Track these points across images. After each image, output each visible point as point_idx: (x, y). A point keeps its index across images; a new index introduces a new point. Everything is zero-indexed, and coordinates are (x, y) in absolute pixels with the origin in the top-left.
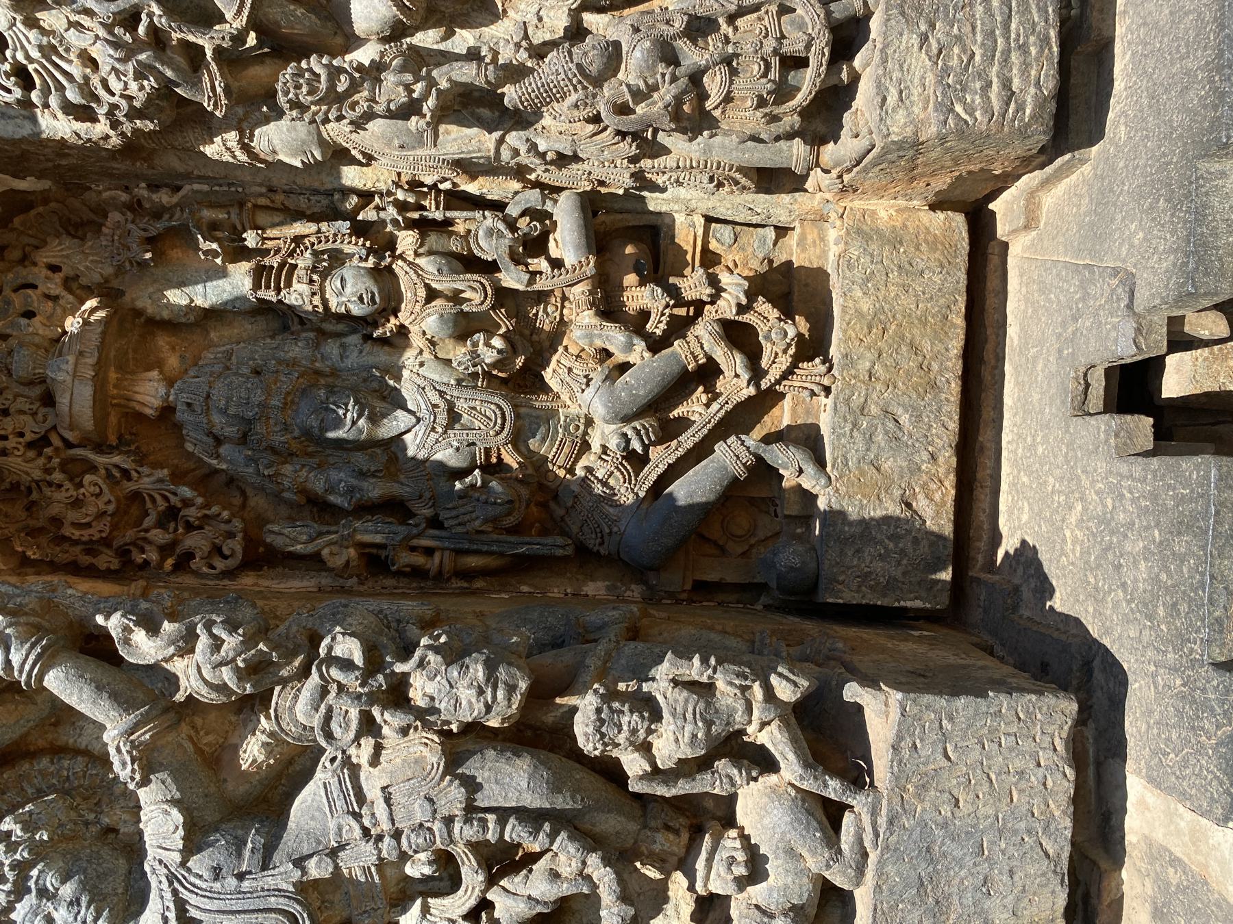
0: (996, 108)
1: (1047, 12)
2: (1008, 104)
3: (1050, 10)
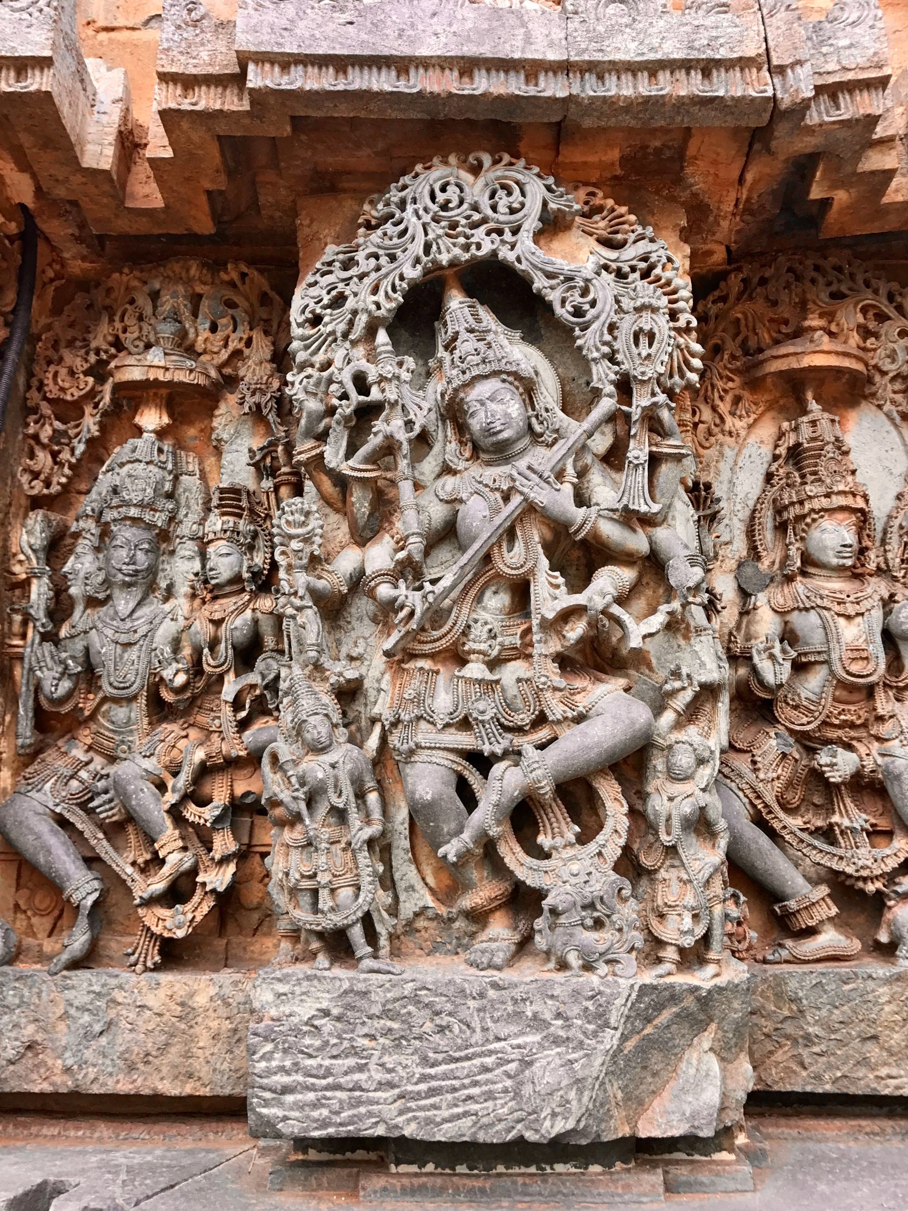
0: (265, 1081)
1: (349, 1124)
2: (270, 1090)
3: (351, 1128)
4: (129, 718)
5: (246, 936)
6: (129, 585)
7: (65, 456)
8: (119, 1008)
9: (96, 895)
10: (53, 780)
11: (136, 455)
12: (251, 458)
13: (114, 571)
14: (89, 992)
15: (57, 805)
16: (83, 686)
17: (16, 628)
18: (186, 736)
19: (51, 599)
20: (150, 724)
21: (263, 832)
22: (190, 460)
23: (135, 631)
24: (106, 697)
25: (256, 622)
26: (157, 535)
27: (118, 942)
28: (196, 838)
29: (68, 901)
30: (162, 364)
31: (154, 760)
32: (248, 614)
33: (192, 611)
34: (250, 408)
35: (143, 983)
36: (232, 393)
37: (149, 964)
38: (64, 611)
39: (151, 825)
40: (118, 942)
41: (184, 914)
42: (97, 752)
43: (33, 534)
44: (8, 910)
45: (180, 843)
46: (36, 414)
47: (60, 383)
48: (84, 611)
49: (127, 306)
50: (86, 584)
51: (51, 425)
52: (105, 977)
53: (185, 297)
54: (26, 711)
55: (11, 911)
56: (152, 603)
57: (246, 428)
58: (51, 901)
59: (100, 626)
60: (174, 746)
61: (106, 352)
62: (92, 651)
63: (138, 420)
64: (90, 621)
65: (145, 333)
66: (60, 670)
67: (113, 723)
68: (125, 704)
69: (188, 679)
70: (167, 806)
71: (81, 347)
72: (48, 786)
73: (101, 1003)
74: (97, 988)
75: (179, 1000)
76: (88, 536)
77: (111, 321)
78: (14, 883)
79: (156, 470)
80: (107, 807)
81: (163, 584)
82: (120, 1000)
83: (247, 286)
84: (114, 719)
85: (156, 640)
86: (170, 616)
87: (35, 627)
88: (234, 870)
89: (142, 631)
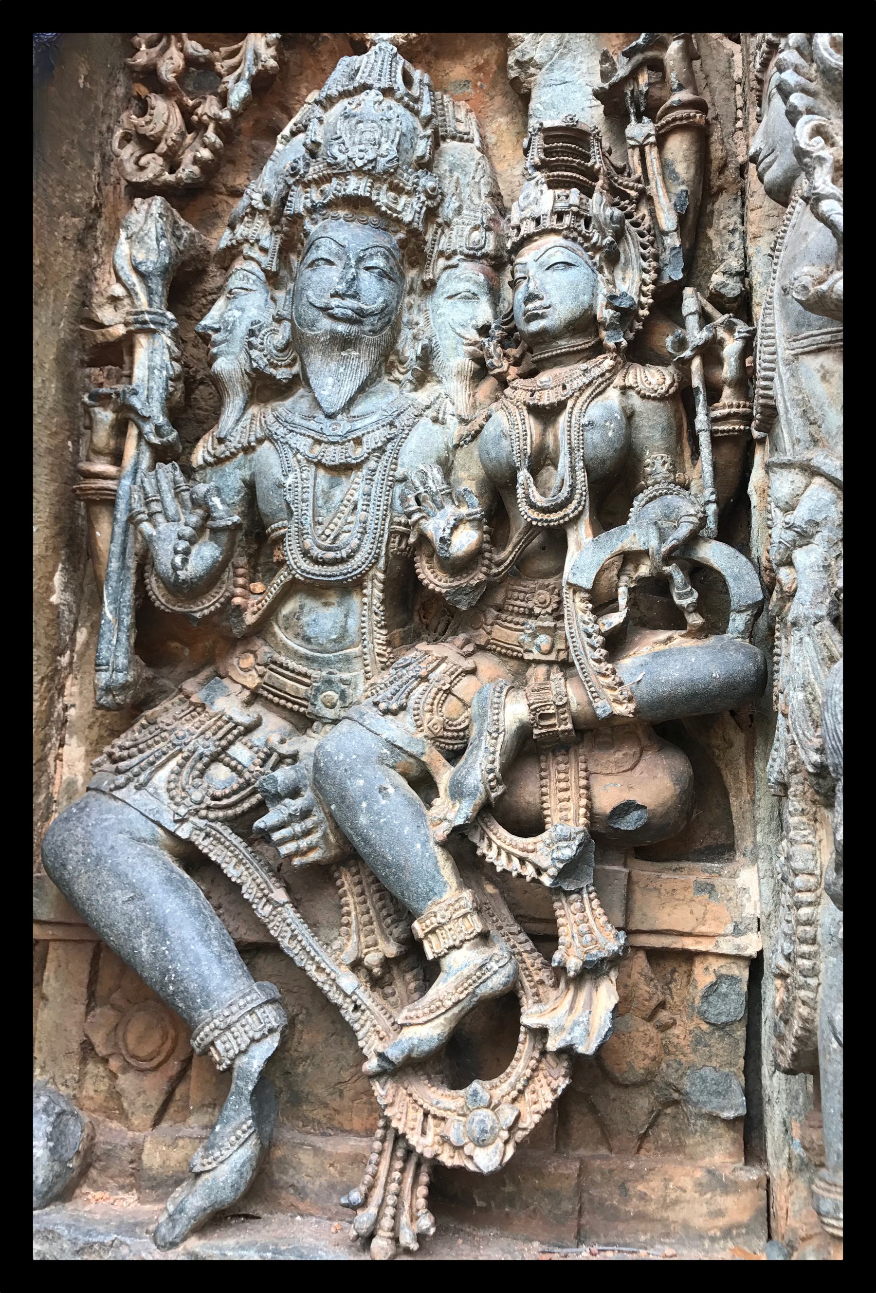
4: (344, 629)
5: (621, 1151)
6: (344, 343)
9: (272, 1043)
10: (173, 765)
15: (182, 821)
16: (243, 561)
17: (102, 437)
18: (473, 672)
19: (175, 379)
20: (389, 643)
21: (653, 899)
22: (461, 115)
23: (358, 441)
24: (294, 581)
25: (630, 416)
26: (400, 241)
27: (316, 1150)
28: (505, 911)
29: (206, 1052)
31: (406, 720)
32: (613, 396)
33: (474, 407)
38: (201, 422)
39: (407, 878)
41: (492, 1106)
42: (269, 704)
43: (141, 241)
44: (68, 1054)
45: (476, 925)
48: (245, 409)
50: (251, 345)
54: (117, 612)
55: (76, 1058)
56: (387, 391)
58: (164, 1037)
59: (281, 431)
60: (448, 692)
62: (263, 486)
64: (257, 427)
66: (194, 519)
67: (308, 640)
68: (334, 599)
69: (481, 541)
70: (442, 832)
72: (162, 777)
76: (256, 253)
78: (82, 991)
79: (400, 109)
80: (298, 828)
81: (411, 351)
84: (309, 632)
85: (404, 458)
86: (431, 413)
87: (141, 435)
88: (614, 1000)
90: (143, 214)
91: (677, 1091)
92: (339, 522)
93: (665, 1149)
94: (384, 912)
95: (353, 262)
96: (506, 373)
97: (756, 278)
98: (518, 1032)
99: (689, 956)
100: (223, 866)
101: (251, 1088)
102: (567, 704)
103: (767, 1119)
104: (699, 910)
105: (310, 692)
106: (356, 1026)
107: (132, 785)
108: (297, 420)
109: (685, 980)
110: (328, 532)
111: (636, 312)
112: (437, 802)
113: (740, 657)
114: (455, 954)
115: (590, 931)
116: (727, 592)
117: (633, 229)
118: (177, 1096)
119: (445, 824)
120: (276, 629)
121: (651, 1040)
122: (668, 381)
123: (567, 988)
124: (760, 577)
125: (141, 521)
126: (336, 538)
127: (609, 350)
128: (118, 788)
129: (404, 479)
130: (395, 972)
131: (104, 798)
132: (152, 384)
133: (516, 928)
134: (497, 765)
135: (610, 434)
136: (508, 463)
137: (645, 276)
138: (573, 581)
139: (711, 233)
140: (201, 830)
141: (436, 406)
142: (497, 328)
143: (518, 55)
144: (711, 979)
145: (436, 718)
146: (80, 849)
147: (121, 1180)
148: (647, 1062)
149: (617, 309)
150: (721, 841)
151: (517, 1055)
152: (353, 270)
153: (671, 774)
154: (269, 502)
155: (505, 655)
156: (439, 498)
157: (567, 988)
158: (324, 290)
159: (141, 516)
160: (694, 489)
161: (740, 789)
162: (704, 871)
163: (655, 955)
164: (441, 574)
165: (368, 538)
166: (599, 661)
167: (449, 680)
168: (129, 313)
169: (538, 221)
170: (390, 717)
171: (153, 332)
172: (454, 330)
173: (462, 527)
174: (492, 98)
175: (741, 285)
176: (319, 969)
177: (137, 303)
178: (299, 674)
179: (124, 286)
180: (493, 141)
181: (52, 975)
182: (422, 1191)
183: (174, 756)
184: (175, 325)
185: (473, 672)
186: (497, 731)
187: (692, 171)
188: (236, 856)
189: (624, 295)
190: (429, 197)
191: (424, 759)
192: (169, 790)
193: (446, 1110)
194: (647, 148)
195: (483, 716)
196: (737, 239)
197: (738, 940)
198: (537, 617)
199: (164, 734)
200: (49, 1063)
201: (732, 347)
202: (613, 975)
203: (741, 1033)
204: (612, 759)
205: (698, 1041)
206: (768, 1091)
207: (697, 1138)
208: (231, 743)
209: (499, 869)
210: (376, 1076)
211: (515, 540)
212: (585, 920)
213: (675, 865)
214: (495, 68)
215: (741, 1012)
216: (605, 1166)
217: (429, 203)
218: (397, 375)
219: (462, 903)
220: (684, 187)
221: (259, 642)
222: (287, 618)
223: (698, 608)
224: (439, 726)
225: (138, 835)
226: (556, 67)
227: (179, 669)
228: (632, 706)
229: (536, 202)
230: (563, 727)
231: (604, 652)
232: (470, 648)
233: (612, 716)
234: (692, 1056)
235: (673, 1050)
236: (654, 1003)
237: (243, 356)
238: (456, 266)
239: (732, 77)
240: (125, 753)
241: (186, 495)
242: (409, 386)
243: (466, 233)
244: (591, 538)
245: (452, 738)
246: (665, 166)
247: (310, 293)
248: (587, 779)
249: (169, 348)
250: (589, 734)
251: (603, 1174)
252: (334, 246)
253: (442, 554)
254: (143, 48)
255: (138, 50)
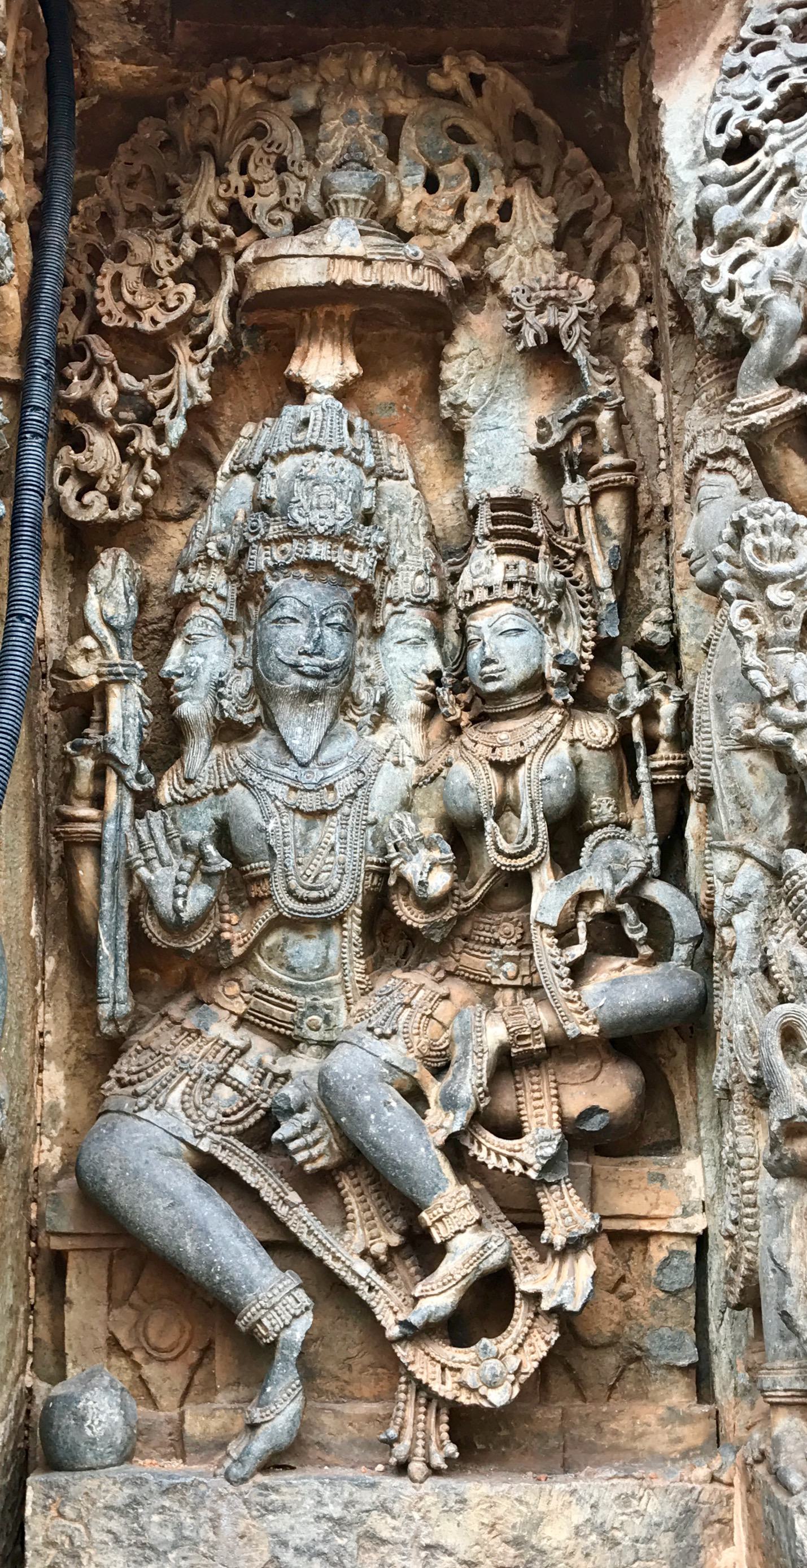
4: (326, 959)
5: (594, 1400)
6: (312, 696)
7: (145, 441)
8: (384, 1549)
10: (182, 1086)
11: (309, 436)
12: (541, 438)
13: (281, 669)
14: (318, 1519)
15: (202, 1136)
18: (446, 997)
21: (613, 1189)
22: (393, 449)
25: (578, 765)
26: (356, 596)
27: (336, 1414)
28: (492, 1203)
30: (358, 251)
31: (398, 1042)
32: (563, 748)
34: (537, 337)
35: (429, 1500)
36: (477, 312)
37: (438, 1460)
40: (336, 1414)
41: (500, 1357)
42: (254, 1027)
44: (96, 1349)
46: (83, 358)
47: (128, 297)
48: (210, 750)
49: (252, 141)
50: (221, 696)
51: (114, 379)
52: (348, 1488)
53: (372, 122)
55: (103, 1354)
56: (347, 734)
57: (513, 381)
58: (182, 1331)
59: (256, 777)
61: (216, 233)
63: (294, 367)
65: (292, 194)
66: (189, 865)
67: (292, 970)
68: (315, 933)
70: (441, 1137)
71: (166, 226)
72: (174, 1098)
73: (347, 1541)
74: (335, 1511)
75: (510, 1534)
76: (213, 601)
77: (221, 172)
79: (349, 466)
80: (310, 1138)
82: (385, 1534)
83: (485, 101)
84: (293, 962)
85: (374, 803)
88: (593, 1268)
89: (346, 785)
90: (109, 569)
91: (640, 1348)
92: (319, 863)
93: (631, 1397)
94: (384, 1209)
95: (317, 621)
96: (460, 719)
97: (684, 629)
98: (514, 1298)
99: (645, 1237)
100: (242, 1174)
101: (295, 1355)
102: (540, 1026)
103: (714, 1366)
104: (652, 1197)
105: (296, 1017)
106: (373, 1304)
107: (152, 1106)
108: (272, 768)
109: (641, 1257)
110: (308, 872)
111: (579, 667)
112: (429, 1112)
113: (685, 983)
114: (460, 1236)
115: (571, 1214)
116: (672, 927)
117: (572, 587)
118: (196, 1381)
119: (443, 1131)
120: (259, 959)
121: (616, 1308)
122: (611, 733)
123: (554, 1261)
124: (699, 913)
125: (139, 866)
126: (316, 877)
127: (557, 706)
128: (141, 1109)
129: (375, 823)
130: (396, 1259)
131: (129, 1119)
132: (128, 732)
133: (502, 1217)
134: (485, 1080)
135: (564, 785)
136: (475, 813)
137: (585, 632)
138: (540, 920)
139: (638, 572)
140: (218, 1143)
141: (394, 748)
142: (448, 675)
143: (451, 398)
144: (665, 1254)
145: (423, 1040)
146: (117, 1164)
147: (162, 1450)
148: (613, 1326)
149: (562, 667)
150: (666, 1138)
151: (515, 1316)
152: (318, 629)
153: (627, 1081)
154: (249, 844)
155: (472, 980)
156: (414, 845)
157: (554, 1261)
158: (293, 648)
159: (138, 862)
160: (635, 828)
161: (683, 1092)
162: (655, 1163)
163: (617, 1237)
164: (416, 911)
165: (348, 878)
166: (567, 989)
167: (430, 1005)
168: (100, 665)
169: (490, 590)
170: (384, 1040)
171: (126, 682)
172: (406, 675)
173: (435, 869)
174: (418, 422)
175: (669, 633)
176: (337, 1259)
177: (109, 655)
178: (284, 1000)
179: (96, 639)
180: (423, 469)
181: (74, 1281)
182: (444, 1427)
183: (182, 1079)
184: (145, 675)
185: (446, 997)
186: (482, 1051)
187: (623, 527)
188: (251, 1165)
189: (567, 652)
190: (379, 551)
191: (416, 1076)
192: (184, 1110)
193: (460, 1362)
194: (582, 508)
195: (466, 1038)
196: (662, 579)
197: (688, 1221)
198: (502, 946)
199: (167, 1059)
200: (79, 1357)
201: (667, 708)
202: (590, 1249)
203: (691, 1298)
204: (578, 1071)
205: (656, 1307)
206: (716, 1343)
207: (658, 1385)
208: (231, 1065)
209: (490, 1167)
210: (399, 1340)
211: (482, 879)
212: (565, 1206)
213: (630, 1159)
214: (420, 391)
215: (691, 1280)
216: (583, 1412)
217: (379, 556)
218: (352, 716)
219: (462, 1195)
220: (616, 542)
221: (243, 971)
222: (270, 949)
223: (647, 941)
224: (426, 1048)
225: (164, 1150)
226: (488, 412)
227: (154, 995)
228: (596, 1028)
229: (488, 571)
230: (537, 1046)
231: (570, 981)
232: (441, 975)
233: (580, 1036)
234: (651, 1320)
235: (633, 1315)
236: (617, 1277)
237: (209, 703)
238: (404, 613)
239: (653, 417)
240: (135, 1078)
241: (177, 841)
242: (368, 730)
243: (411, 579)
244: (552, 880)
245: (437, 1056)
246: (599, 521)
247: (278, 650)
248: (556, 1088)
249: (140, 697)
250: (556, 1051)
251: (581, 1417)
252: (299, 605)
253: (421, 895)
254: (76, 380)
255: (71, 381)
